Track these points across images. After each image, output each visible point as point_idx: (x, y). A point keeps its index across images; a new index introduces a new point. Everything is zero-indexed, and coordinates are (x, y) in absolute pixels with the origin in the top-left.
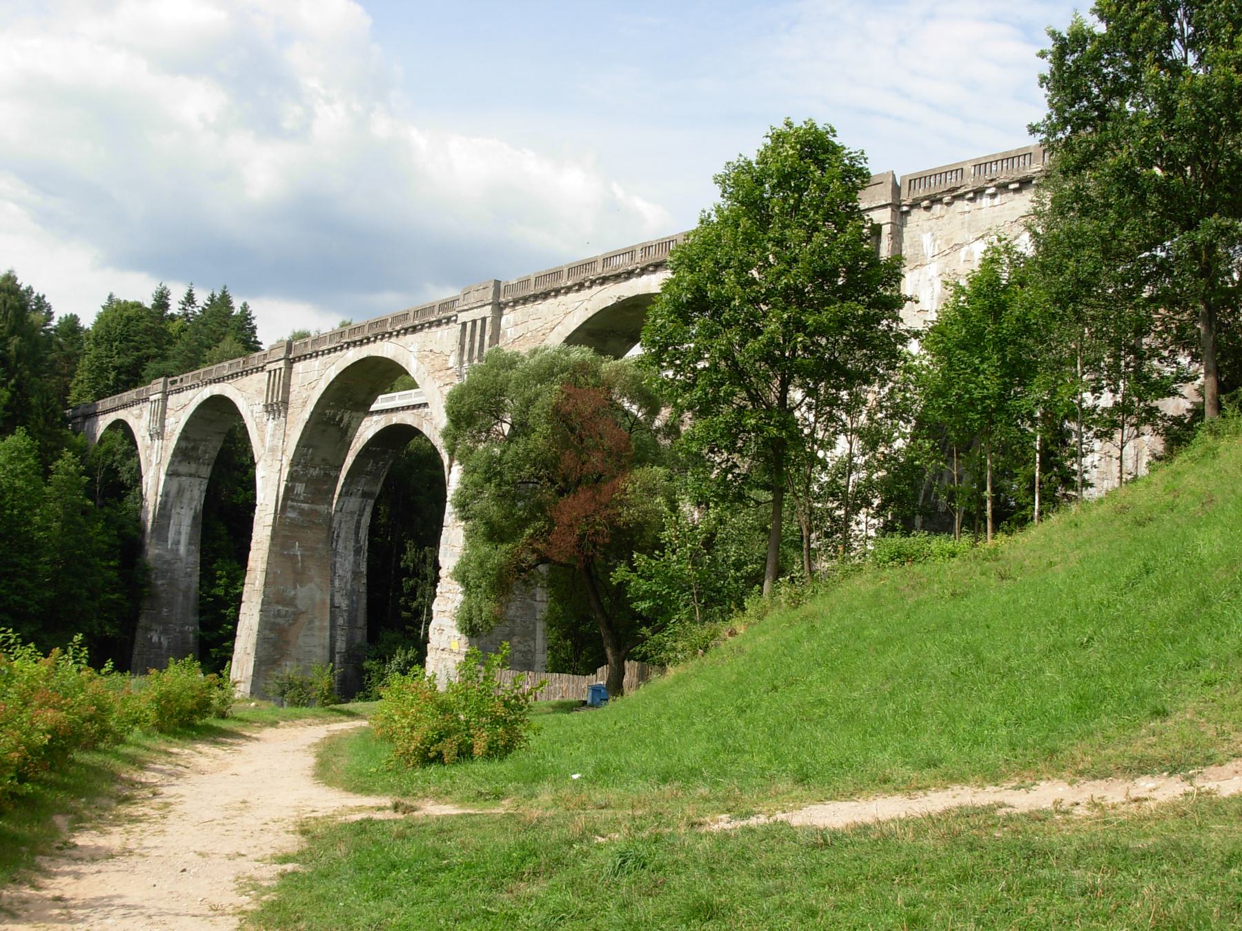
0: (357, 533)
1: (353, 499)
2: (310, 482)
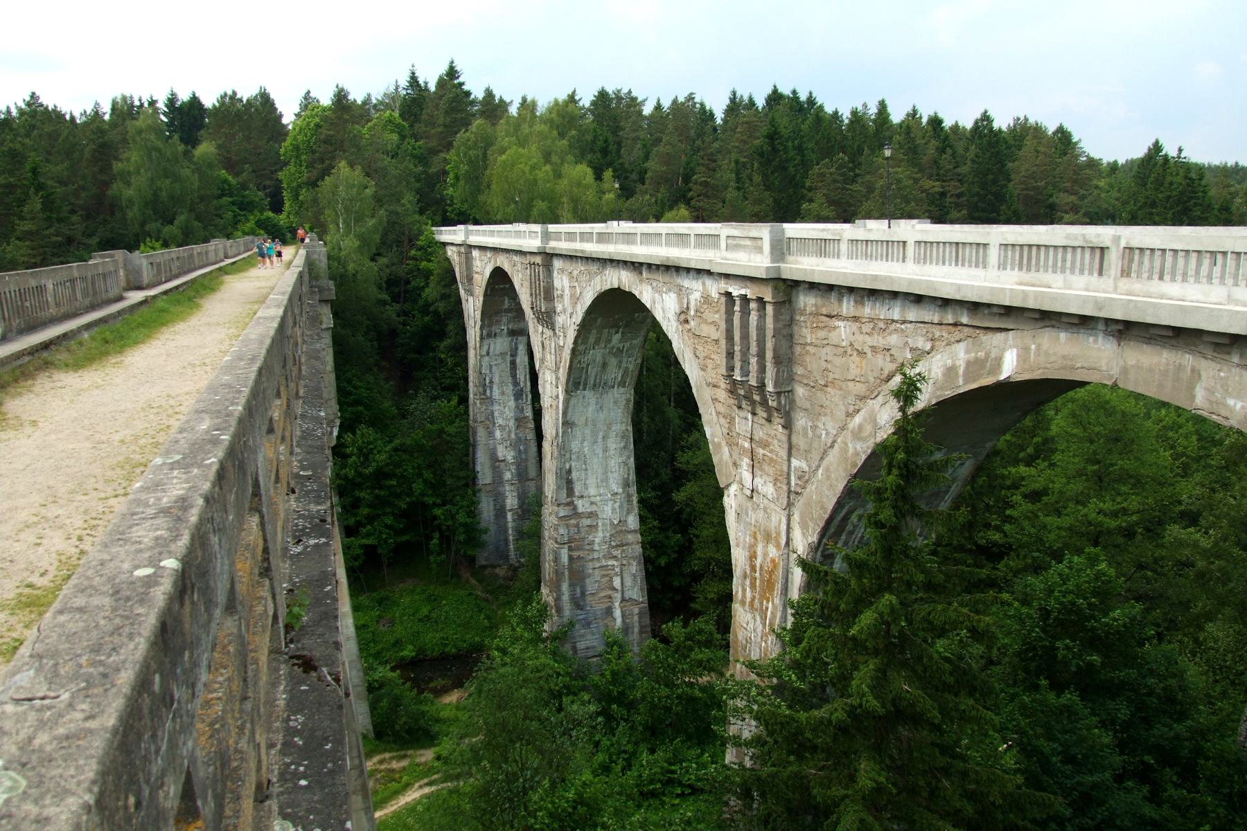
0: (514, 376)
1: (499, 340)
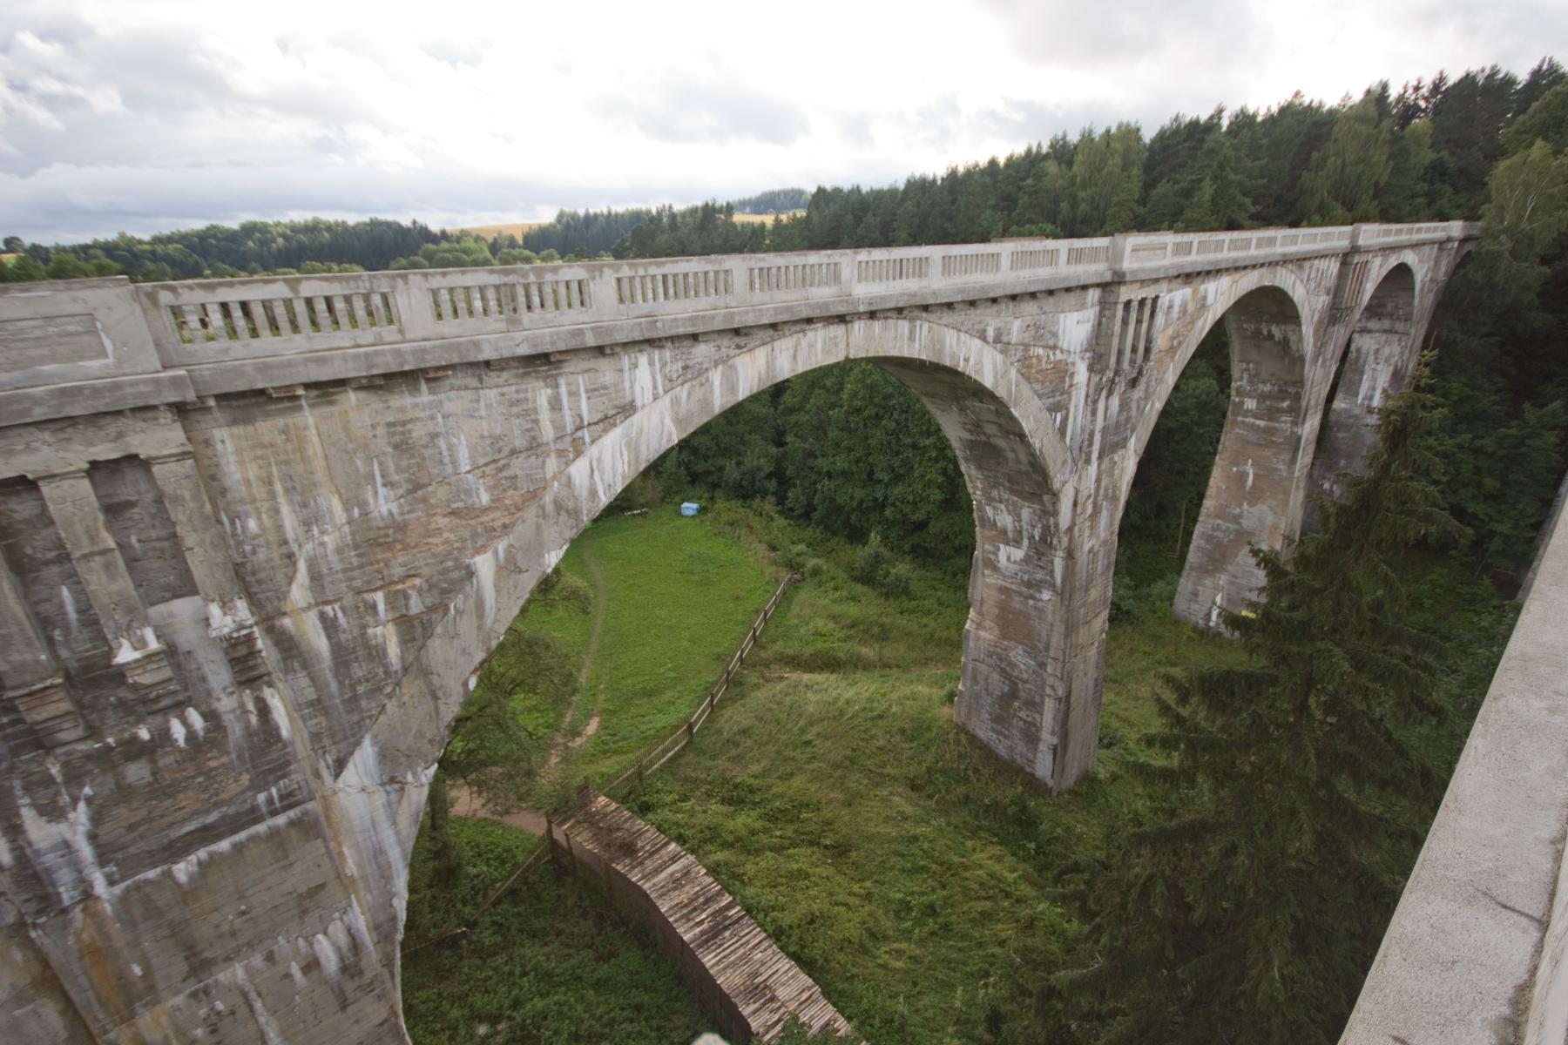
2: (1262, 397)
